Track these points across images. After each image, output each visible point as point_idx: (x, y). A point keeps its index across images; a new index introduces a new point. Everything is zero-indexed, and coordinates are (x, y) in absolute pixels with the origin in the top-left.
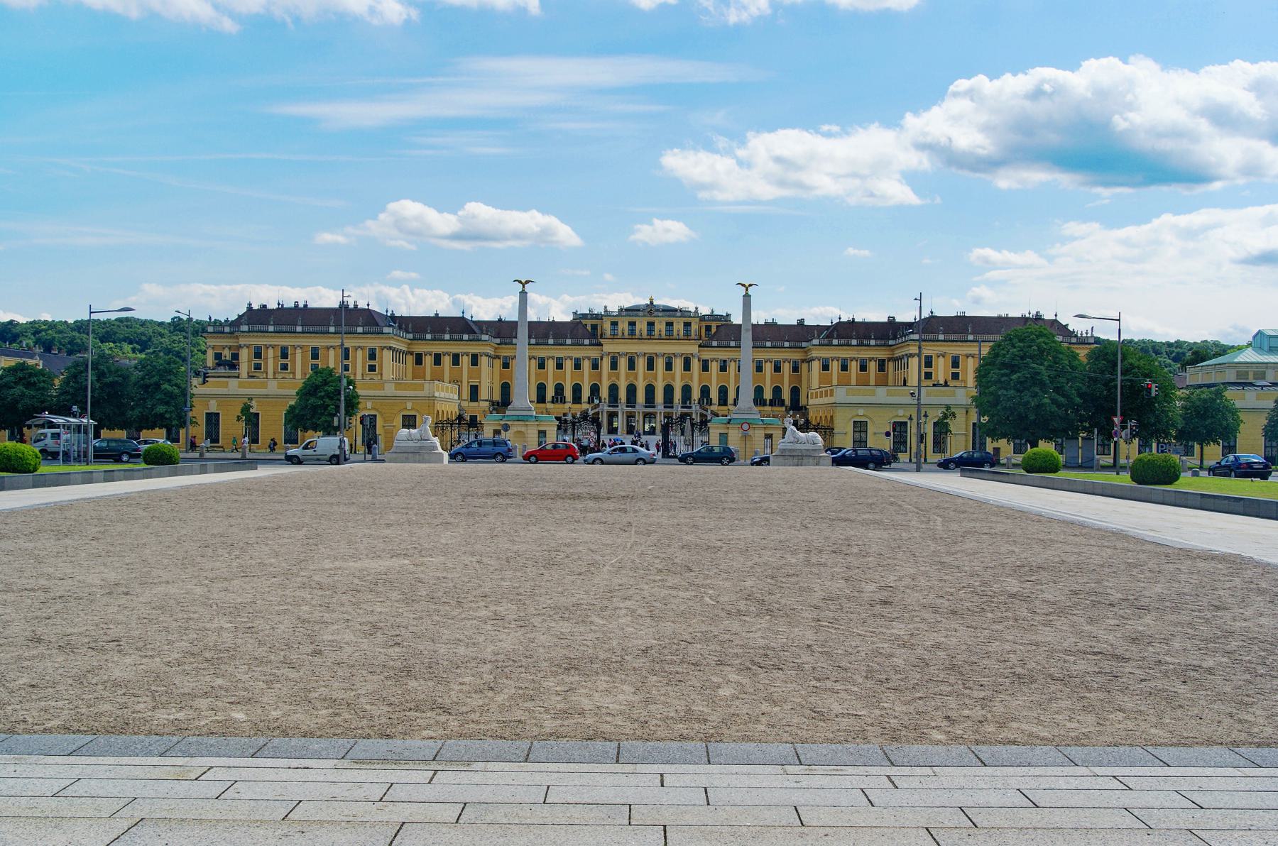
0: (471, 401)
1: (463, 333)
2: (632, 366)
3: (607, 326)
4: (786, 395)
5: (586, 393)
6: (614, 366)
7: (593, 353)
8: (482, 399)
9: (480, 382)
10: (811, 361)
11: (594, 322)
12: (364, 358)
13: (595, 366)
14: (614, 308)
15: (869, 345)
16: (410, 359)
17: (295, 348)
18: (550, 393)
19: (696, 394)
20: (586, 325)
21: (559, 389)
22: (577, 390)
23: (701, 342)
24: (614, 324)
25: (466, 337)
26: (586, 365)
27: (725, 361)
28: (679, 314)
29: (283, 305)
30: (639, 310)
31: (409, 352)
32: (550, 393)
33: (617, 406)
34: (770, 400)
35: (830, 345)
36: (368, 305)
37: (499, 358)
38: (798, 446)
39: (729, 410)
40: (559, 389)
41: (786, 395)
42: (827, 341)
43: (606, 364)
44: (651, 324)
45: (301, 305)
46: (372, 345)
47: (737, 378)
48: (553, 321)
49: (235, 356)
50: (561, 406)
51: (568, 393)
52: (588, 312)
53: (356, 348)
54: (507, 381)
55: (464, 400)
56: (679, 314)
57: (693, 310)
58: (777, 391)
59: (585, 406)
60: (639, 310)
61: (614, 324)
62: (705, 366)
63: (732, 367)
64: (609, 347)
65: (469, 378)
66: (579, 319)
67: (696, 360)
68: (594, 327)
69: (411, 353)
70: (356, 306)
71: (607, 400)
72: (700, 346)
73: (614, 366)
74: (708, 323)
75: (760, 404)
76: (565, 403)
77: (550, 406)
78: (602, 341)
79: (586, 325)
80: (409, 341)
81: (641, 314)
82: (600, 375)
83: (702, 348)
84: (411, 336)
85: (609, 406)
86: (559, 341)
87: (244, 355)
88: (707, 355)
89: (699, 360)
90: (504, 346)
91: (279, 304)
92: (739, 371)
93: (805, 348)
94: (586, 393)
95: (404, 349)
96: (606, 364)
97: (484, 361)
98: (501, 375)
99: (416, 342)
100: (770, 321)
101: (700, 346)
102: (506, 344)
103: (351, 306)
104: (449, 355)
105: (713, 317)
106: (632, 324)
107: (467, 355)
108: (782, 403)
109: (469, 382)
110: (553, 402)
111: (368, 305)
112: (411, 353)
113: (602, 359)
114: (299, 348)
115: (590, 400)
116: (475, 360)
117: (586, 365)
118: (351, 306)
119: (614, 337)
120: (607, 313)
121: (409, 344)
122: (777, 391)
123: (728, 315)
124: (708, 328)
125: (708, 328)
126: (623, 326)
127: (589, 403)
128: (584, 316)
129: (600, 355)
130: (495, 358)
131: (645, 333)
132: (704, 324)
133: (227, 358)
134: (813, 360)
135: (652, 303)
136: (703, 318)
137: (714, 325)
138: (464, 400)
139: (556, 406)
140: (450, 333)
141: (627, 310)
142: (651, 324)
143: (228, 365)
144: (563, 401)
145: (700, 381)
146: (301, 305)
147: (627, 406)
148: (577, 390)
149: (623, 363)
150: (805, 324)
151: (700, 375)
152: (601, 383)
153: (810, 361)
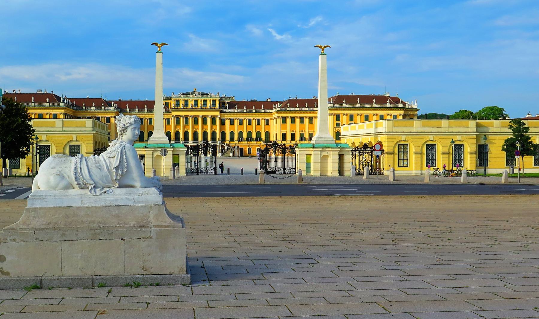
4: (263, 136)
28: (209, 96)
30: (190, 95)
31: (74, 116)
35: (286, 110)
36: (52, 92)
39: (236, 143)
41: (263, 136)
42: (284, 109)
58: (259, 134)
72: (220, 112)
75: (259, 140)
80: (74, 111)
83: (221, 113)
95: (71, 114)
99: (77, 111)
108: (261, 140)
111: (52, 92)
113: (172, 119)
121: (74, 112)
122: (259, 134)
146: (17, 92)
152: (171, 131)
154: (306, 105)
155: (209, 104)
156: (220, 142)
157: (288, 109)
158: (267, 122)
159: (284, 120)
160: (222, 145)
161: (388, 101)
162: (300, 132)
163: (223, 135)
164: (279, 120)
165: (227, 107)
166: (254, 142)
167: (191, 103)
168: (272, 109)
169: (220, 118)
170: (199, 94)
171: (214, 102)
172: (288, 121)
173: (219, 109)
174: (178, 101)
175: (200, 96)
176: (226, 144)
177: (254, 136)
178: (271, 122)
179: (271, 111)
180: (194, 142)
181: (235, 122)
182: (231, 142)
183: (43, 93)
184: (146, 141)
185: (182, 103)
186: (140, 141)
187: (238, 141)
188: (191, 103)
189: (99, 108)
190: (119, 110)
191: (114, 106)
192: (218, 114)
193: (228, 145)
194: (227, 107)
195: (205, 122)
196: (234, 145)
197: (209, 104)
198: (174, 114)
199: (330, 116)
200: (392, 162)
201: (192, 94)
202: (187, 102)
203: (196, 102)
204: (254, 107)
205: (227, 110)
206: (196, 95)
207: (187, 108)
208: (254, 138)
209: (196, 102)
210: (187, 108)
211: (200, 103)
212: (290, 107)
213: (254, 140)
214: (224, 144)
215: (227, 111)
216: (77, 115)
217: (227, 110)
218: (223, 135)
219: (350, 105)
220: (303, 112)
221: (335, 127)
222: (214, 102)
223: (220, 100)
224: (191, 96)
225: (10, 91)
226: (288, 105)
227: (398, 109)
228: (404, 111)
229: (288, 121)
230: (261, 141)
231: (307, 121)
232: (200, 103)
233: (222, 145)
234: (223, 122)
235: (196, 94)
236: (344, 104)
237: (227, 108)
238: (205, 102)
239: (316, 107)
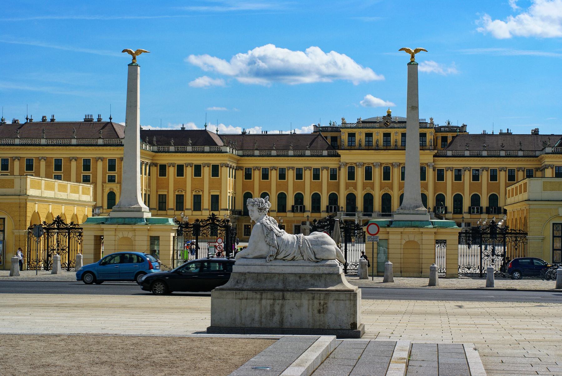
0: (177, 210)
1: (205, 145)
2: (368, 175)
3: (345, 137)
5: (324, 202)
6: (351, 175)
7: (332, 163)
8: (222, 208)
10: (544, 169)
11: (334, 134)
12: (104, 169)
13: (334, 176)
14: (352, 120)
17: (39, 159)
18: (290, 202)
19: (342, 202)
20: (326, 137)
21: (299, 198)
22: (316, 199)
23: (436, 151)
24: (352, 135)
25: (207, 148)
26: (325, 175)
27: (459, 170)
29: (31, 120)
31: (154, 163)
32: (290, 202)
33: (354, 215)
34: (487, 208)
37: (242, 170)
38: (278, 268)
39: (463, 217)
40: (299, 198)
43: (343, 174)
44: (387, 135)
45: (48, 119)
46: (86, 156)
48: (294, 133)
50: (300, 214)
51: (308, 202)
52: (329, 125)
53: (97, 160)
54: (250, 192)
55: (206, 210)
57: (428, 121)
60: (375, 122)
61: (352, 135)
62: (440, 175)
64: (347, 157)
65: (210, 188)
66: (319, 130)
67: (431, 170)
68: (334, 139)
69: (156, 165)
70: (99, 120)
71: (344, 209)
72: (435, 156)
73: (351, 175)
74: (444, 134)
76: (304, 211)
77: (290, 215)
78: (340, 152)
79: (326, 137)
81: (377, 125)
82: (338, 185)
84: (155, 148)
85: (347, 215)
86: (299, 153)
88: (442, 163)
89: (434, 170)
91: (27, 119)
92: (403, 179)
93: (538, 157)
94: (324, 202)
96: (343, 174)
97: (225, 172)
98: (244, 185)
100: (505, 131)
101: (435, 156)
102: (248, 156)
103: (95, 120)
104: (174, 166)
105: (450, 129)
106: (369, 135)
107: (208, 166)
109: (157, 192)
110: (293, 211)
111: (111, 119)
112: (156, 165)
113: (340, 170)
114: (43, 160)
115: (328, 209)
116: (215, 171)
117: (325, 175)
118: (95, 120)
119: (351, 147)
120: (345, 125)
121: (154, 156)
123: (464, 126)
124: (444, 139)
125: (444, 139)
126: (360, 136)
127: (327, 211)
128: (325, 129)
129: (338, 166)
131: (381, 142)
132: (440, 135)
134: (546, 167)
135: (389, 115)
136: (438, 129)
137: (450, 135)
138: (206, 210)
139: (297, 214)
140: (193, 145)
141: (363, 122)
142: (387, 135)
144: (303, 210)
145: (435, 190)
146: (48, 119)
147: (364, 215)
148: (316, 199)
149: (360, 173)
150: (540, 133)
151: (435, 184)
152: (339, 193)
153: (543, 169)
166: (485, 216)
177: (484, 203)
183: (9, 122)
184: (289, 211)
216: (158, 162)
225: (37, 119)
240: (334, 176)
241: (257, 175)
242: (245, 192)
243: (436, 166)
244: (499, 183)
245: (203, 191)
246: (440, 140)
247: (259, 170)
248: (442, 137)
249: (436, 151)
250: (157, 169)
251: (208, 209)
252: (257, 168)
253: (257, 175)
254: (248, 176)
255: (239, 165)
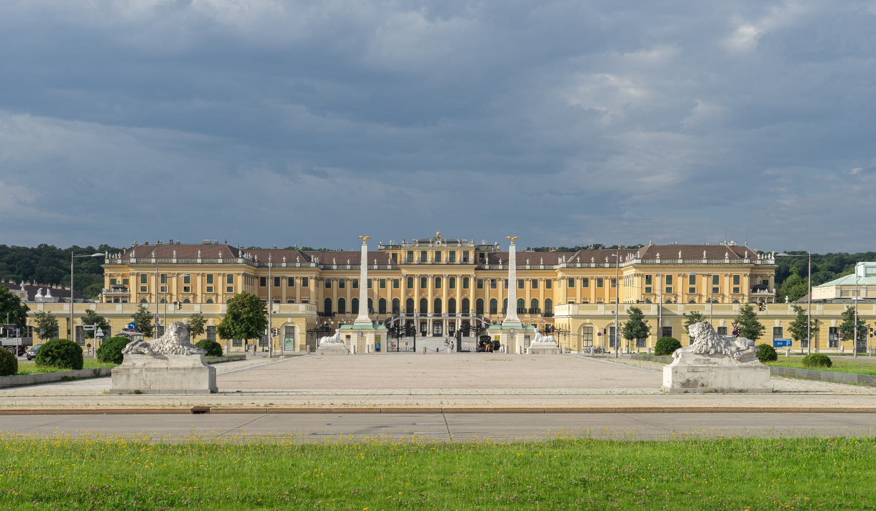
4: (542, 306)
9: (309, 298)
11: (395, 251)
13: (396, 284)
15: (603, 267)
16: (257, 282)
20: (388, 254)
23: (477, 266)
28: (459, 245)
34: (529, 309)
35: (575, 267)
37: (323, 280)
39: (498, 317)
41: (542, 306)
43: (402, 284)
47: (505, 293)
49: (126, 282)
56: (459, 245)
58: (535, 302)
59: (389, 316)
63: (500, 284)
65: (301, 296)
69: (257, 277)
72: (476, 269)
76: (373, 313)
79: (388, 254)
83: (478, 271)
87: (132, 280)
88: (482, 275)
90: (326, 271)
95: (252, 274)
96: (402, 284)
99: (261, 269)
101: (476, 269)
104: (286, 279)
112: (257, 277)
113: (401, 280)
121: (256, 271)
122: (535, 302)
130: (320, 280)
133: (120, 283)
143: (121, 288)
154: (607, 259)
155: (459, 257)
156: (475, 315)
157: (578, 265)
158: (549, 284)
159: (571, 282)
160: (477, 320)
161: (727, 254)
162: (597, 300)
163: (480, 304)
164: (564, 283)
165: (487, 261)
167: (430, 256)
168: (557, 264)
169: (475, 279)
170: (443, 242)
171: (466, 254)
172: (578, 283)
173: (474, 264)
174: (411, 253)
175: (445, 245)
176: (483, 318)
178: (555, 284)
179: (555, 267)
180: (435, 316)
181: (484, 285)
182: (493, 316)
185: (417, 256)
186: (339, 313)
187: (503, 313)
188: (430, 256)
189: (292, 264)
190: (322, 267)
191: (314, 260)
192: (472, 273)
193: (486, 320)
194: (487, 261)
195: (452, 284)
196: (496, 320)
197: (459, 257)
198: (404, 272)
199: (637, 278)
200: (577, 343)
201: (433, 242)
202: (424, 254)
203: (438, 254)
204: (528, 261)
205: (486, 266)
206: (438, 244)
207: (425, 263)
208: (528, 309)
209: (438, 254)
210: (425, 263)
211: (445, 257)
212: (581, 262)
213: (528, 311)
214: (481, 318)
215: (487, 267)
217: (486, 266)
218: (480, 304)
219: (667, 261)
220: (601, 269)
221: (643, 294)
222: (466, 254)
223: (477, 249)
224: (430, 245)
226: (578, 259)
227: (742, 266)
228: (752, 268)
229: (578, 283)
230: (539, 313)
231: (607, 283)
232: (445, 257)
233: (477, 320)
234: (480, 285)
235: (439, 242)
236: (658, 259)
237: (487, 264)
238: (453, 254)
239: (621, 263)
240: (396, 284)
241: (335, 285)
242: (477, 299)
243: (477, 277)
244: (525, 290)
245: (295, 298)
246: (479, 256)
247: (337, 280)
248: (480, 254)
249: (477, 266)
250: (259, 280)
251: (390, 313)
252: (375, 279)
253: (335, 285)
254: (328, 285)
255: (321, 277)
